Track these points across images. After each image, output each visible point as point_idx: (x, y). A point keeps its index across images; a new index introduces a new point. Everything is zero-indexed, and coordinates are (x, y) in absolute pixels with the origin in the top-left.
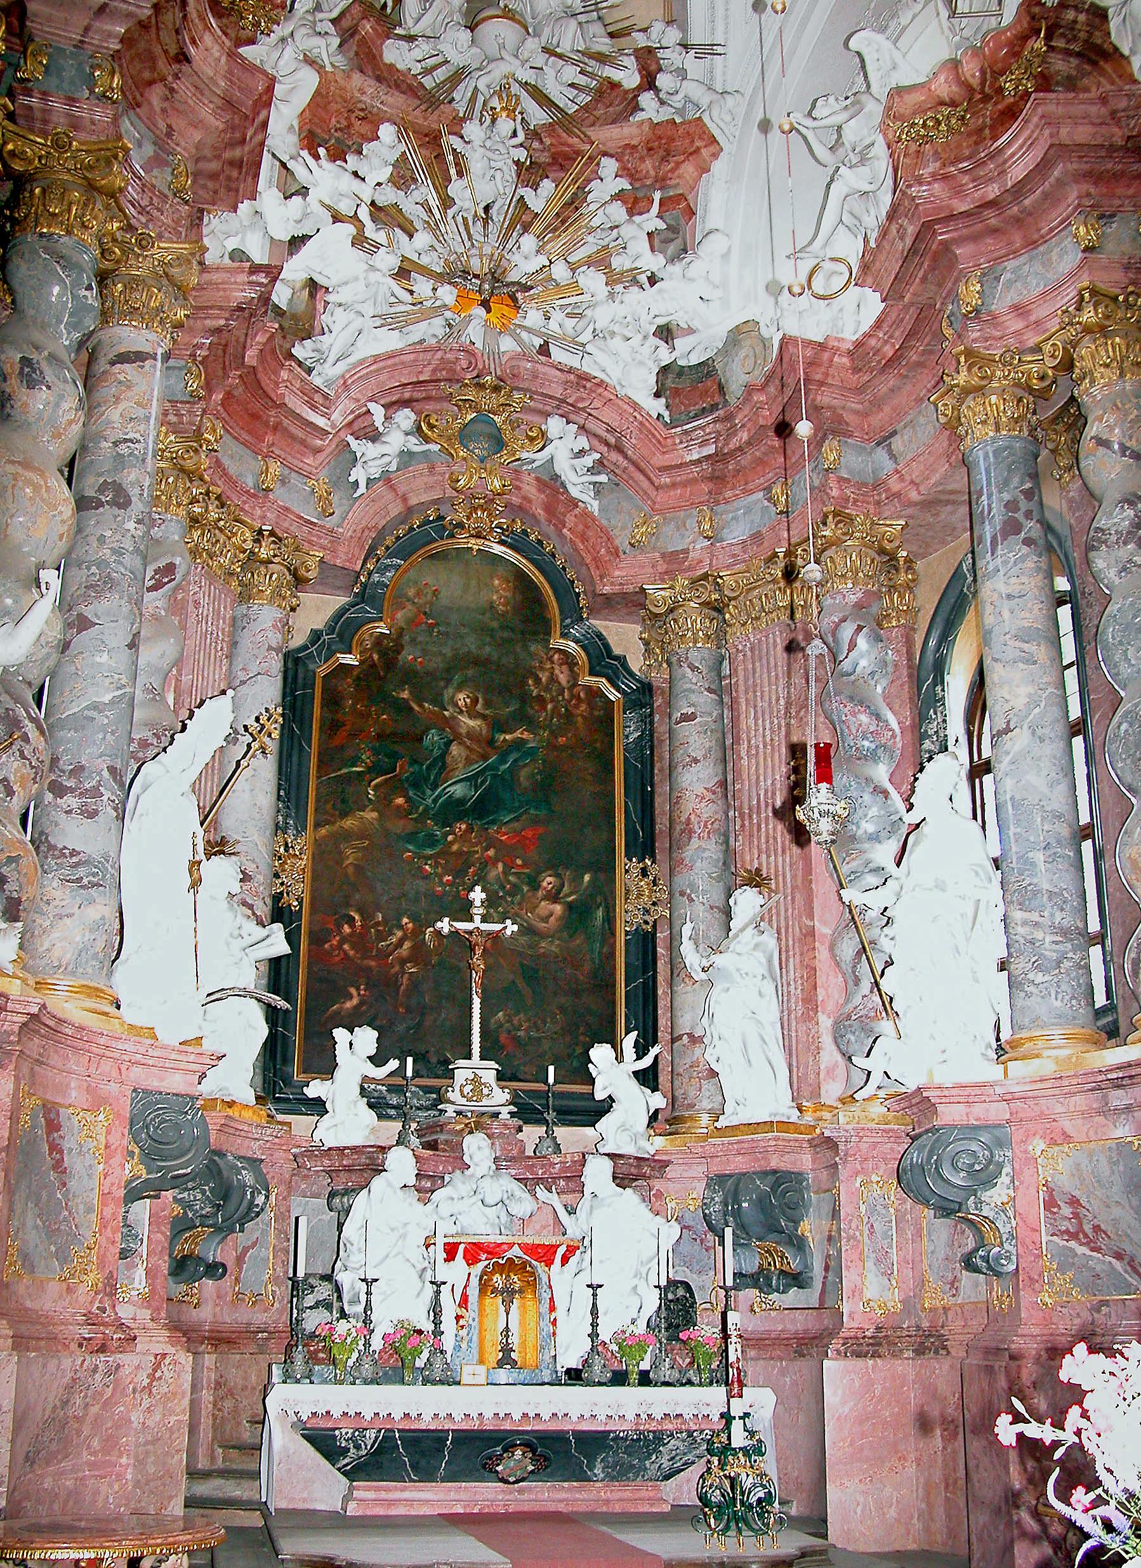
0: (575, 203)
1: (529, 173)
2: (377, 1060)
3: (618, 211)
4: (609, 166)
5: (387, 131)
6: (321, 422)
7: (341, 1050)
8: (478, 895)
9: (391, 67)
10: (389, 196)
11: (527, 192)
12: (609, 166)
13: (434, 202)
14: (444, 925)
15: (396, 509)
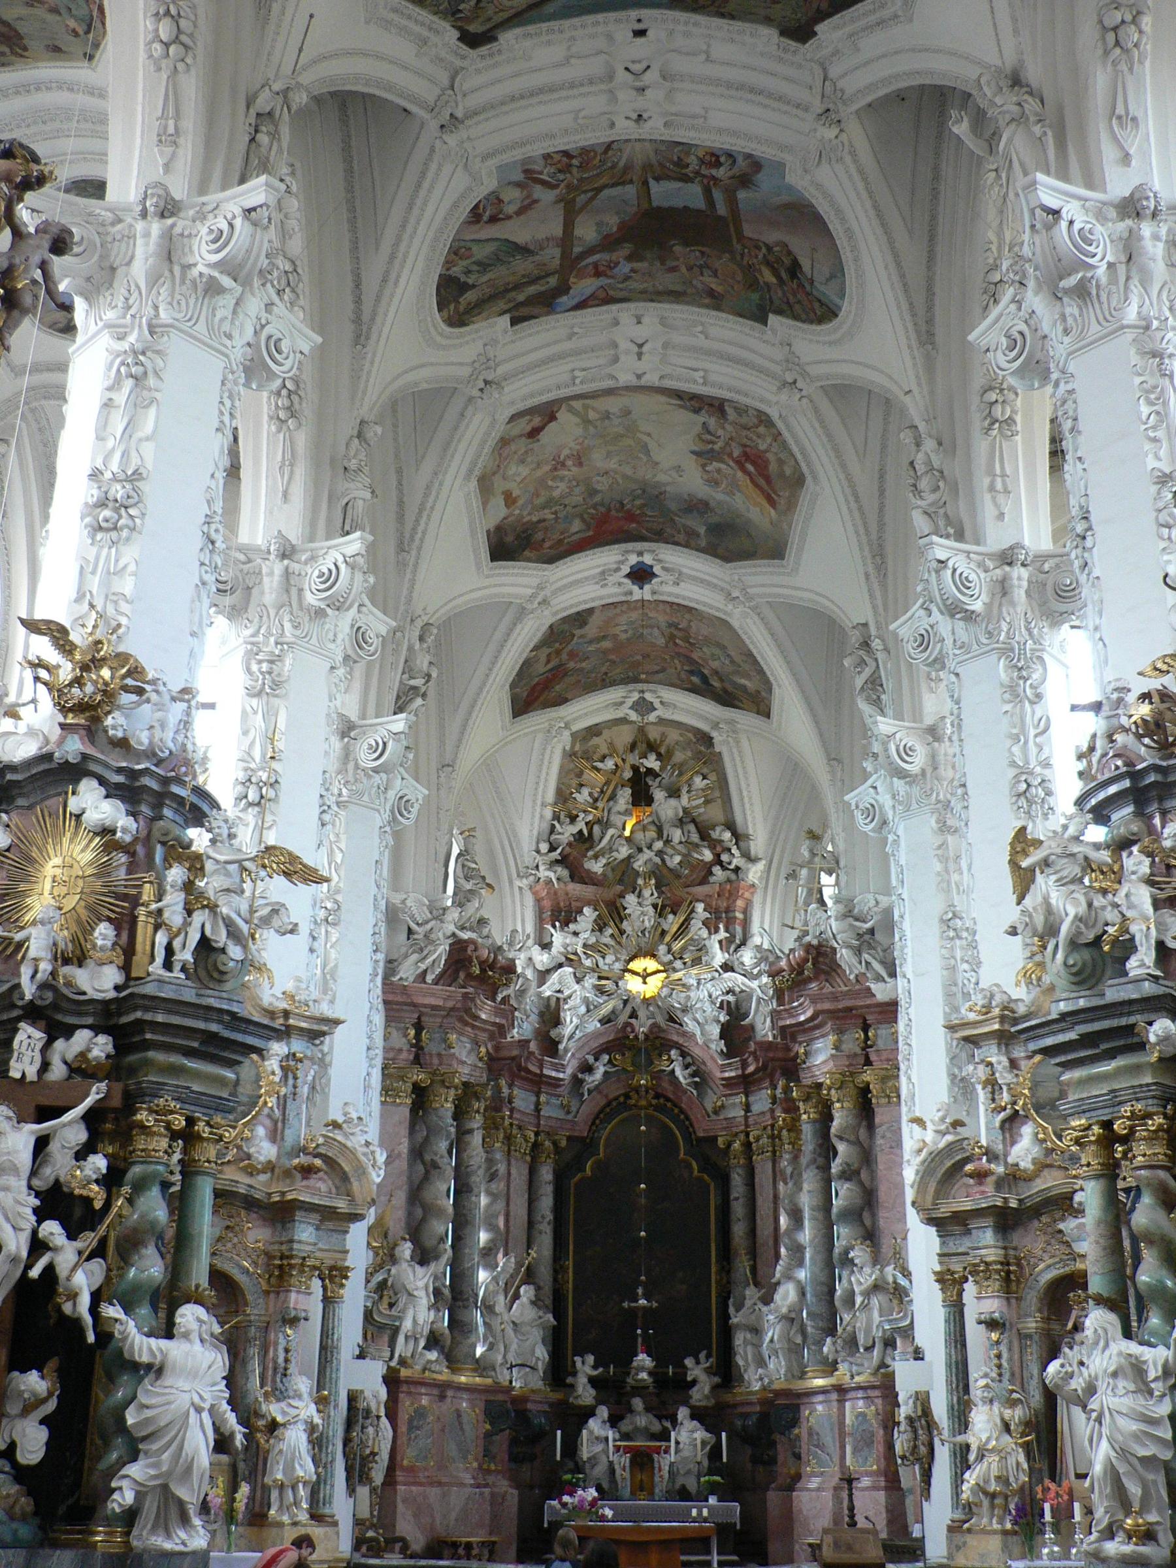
0: (684, 927)
1: (659, 912)
2: (595, 1367)
3: (704, 933)
4: (700, 907)
5: (586, 910)
6: (561, 1076)
7: (579, 1364)
8: (640, 1291)
9: (588, 871)
10: (593, 940)
11: (661, 920)
12: (700, 907)
14: (625, 1305)
15: (603, 1102)
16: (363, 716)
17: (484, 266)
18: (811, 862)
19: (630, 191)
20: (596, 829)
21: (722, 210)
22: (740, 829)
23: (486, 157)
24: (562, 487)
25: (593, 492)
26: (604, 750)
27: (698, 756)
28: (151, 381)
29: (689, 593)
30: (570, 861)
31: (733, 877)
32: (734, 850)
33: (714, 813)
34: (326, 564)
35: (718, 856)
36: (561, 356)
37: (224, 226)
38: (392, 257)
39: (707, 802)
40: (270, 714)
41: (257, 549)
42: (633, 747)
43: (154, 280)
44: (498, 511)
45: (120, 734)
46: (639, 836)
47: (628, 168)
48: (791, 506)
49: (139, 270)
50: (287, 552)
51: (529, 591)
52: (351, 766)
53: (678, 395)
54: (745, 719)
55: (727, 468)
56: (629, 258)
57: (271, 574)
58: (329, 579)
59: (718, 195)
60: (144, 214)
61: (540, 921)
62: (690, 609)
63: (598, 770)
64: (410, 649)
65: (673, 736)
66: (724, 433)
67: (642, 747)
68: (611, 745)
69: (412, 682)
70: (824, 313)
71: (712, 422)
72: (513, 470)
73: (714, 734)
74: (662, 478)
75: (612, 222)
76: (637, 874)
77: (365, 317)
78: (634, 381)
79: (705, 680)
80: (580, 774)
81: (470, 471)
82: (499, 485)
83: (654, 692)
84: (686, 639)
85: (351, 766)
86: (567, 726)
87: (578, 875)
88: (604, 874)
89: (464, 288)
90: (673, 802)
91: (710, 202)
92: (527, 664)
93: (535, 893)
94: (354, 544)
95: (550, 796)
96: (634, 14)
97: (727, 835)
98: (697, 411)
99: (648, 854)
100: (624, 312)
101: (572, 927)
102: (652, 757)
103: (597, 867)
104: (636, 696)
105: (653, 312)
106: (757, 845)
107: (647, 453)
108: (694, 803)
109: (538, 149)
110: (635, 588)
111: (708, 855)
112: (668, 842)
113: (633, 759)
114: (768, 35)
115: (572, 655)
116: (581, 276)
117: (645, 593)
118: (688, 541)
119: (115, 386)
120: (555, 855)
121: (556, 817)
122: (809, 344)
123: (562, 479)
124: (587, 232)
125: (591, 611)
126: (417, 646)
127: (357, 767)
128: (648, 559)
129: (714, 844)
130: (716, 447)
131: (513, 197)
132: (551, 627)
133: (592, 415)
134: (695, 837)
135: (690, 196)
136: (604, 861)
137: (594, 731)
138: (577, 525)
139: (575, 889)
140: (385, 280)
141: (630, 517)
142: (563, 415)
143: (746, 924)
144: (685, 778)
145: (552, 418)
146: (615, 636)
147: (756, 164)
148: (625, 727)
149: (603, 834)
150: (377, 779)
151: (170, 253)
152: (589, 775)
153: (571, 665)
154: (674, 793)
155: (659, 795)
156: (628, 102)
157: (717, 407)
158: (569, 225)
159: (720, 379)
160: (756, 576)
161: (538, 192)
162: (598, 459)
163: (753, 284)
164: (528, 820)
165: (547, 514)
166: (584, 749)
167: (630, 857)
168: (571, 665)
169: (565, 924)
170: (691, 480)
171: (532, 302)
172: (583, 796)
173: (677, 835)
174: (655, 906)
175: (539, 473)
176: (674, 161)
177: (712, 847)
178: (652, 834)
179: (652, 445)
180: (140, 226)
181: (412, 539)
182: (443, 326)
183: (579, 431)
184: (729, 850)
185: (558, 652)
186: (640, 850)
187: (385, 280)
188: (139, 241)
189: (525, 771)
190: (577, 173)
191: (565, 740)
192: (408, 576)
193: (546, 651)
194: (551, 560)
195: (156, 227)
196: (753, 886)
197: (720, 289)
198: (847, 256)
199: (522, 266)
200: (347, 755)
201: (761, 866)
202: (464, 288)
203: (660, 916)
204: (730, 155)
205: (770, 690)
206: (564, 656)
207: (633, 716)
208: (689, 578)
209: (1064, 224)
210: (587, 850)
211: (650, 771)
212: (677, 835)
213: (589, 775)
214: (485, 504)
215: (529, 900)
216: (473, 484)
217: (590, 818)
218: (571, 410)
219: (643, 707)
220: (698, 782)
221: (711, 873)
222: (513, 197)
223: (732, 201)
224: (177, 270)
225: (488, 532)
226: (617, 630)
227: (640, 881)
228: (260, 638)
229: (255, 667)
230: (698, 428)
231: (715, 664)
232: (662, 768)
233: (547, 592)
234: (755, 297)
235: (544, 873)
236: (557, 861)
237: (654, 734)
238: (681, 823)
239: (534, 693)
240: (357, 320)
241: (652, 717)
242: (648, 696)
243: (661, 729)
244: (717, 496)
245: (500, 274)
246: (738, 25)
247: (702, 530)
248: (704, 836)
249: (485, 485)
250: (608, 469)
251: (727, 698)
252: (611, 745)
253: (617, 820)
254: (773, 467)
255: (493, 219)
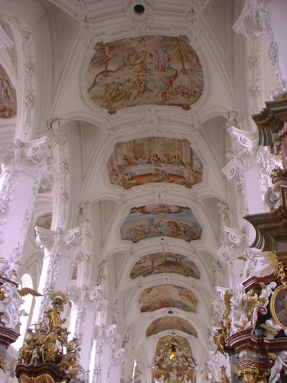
1: (178, 376)
4: (186, 375)
5: (162, 375)
9: (163, 367)
12: (186, 375)
13: (169, 381)
16: (116, 348)
17: (138, 270)
18: (205, 370)
19: (163, 258)
20: (164, 358)
21: (179, 261)
22: (194, 358)
23: (137, 256)
24: (154, 299)
25: (160, 300)
26: (166, 341)
27: (185, 343)
28: (84, 318)
29: (180, 315)
30: (159, 365)
31: (192, 369)
32: (193, 363)
33: (188, 355)
34: (110, 330)
35: (189, 364)
36: (153, 281)
37: (95, 292)
38: (122, 272)
39: (187, 352)
40: (100, 357)
41: (98, 326)
42: (172, 341)
43: (84, 300)
44: (142, 305)
45: (78, 378)
46: (173, 359)
47: (162, 255)
48: (196, 305)
49: (82, 298)
50: (103, 327)
51: (148, 316)
52: (114, 358)
53: (175, 286)
54: (193, 337)
55: (185, 297)
56: (163, 267)
57: (100, 331)
58: (110, 332)
59: (178, 260)
60: (83, 289)
61: (153, 377)
62: (180, 318)
63: (165, 345)
64: (125, 333)
65: (180, 339)
66: (183, 292)
67: (174, 341)
68: (167, 340)
69: (126, 340)
70: (198, 278)
71: (181, 290)
72: (145, 298)
73: (187, 339)
74: (172, 297)
75: (160, 263)
76: (173, 368)
77: (117, 282)
78: (166, 284)
79: (185, 329)
80: (161, 346)
81: (137, 300)
82: (142, 301)
83: (175, 331)
84: (180, 322)
85: (114, 358)
86: (158, 337)
87: (161, 368)
88: (166, 368)
89: (134, 274)
90: (180, 352)
91: (177, 260)
92: (149, 328)
93: (152, 372)
94: (114, 326)
95: (155, 351)
96: (161, 237)
97: (191, 360)
98: (178, 288)
99: (175, 363)
100: (164, 274)
101: (159, 379)
102: (176, 343)
103: (164, 366)
104: (172, 332)
105: (168, 274)
106: (198, 362)
107: (170, 294)
108: (185, 352)
109: (147, 254)
110: (170, 314)
111: (187, 364)
112: (179, 361)
113: (172, 343)
114: (184, 241)
115: (158, 325)
116: (155, 269)
117: (172, 315)
118: (179, 307)
119: (78, 318)
120: (156, 363)
121: (156, 355)
122: (196, 281)
123: (154, 298)
124: (156, 264)
125: (161, 318)
126: (127, 332)
127: (115, 358)
128: (171, 310)
129: (189, 362)
130: (182, 293)
131: (142, 260)
132: (154, 321)
133: (159, 289)
134: (185, 360)
135: (174, 259)
136: (166, 365)
137: (164, 338)
138: (157, 305)
139: (160, 371)
140: (121, 276)
141: (167, 303)
142: (153, 289)
143: (195, 379)
144: (183, 347)
145: (152, 290)
146: (167, 322)
147: (184, 256)
148: (170, 337)
149: (166, 359)
150: (119, 360)
151: (87, 296)
152: (163, 346)
153: (158, 327)
154: (180, 350)
155: (177, 350)
156: (161, 248)
157: (182, 288)
158: (153, 263)
159: (181, 284)
160: (191, 314)
161: (147, 259)
162: (161, 295)
163: (186, 272)
164: (150, 356)
165: (152, 304)
166: (161, 342)
167: (171, 364)
168: (158, 327)
169: (158, 378)
170: (178, 298)
171: (147, 273)
172: (162, 351)
173: (181, 359)
174: (176, 375)
175: (150, 298)
176: (170, 255)
177: (188, 363)
178: (176, 359)
179: (170, 293)
180: (82, 291)
181: (126, 312)
182: (131, 280)
183: (157, 291)
184: (191, 363)
185: (155, 325)
186: (173, 362)
187: (121, 276)
188: (82, 294)
189: (150, 346)
190: (153, 257)
191: (158, 340)
192: (125, 320)
193: (153, 325)
194: (153, 311)
195: (85, 292)
196: (197, 371)
197: (180, 272)
198: (200, 270)
199: (145, 269)
200: (113, 355)
201: (198, 367)
202: (134, 274)
203: (178, 376)
204: (179, 255)
205: (197, 333)
206: (157, 326)
207: (171, 335)
208: (179, 313)
209: (221, 294)
210: (163, 362)
211: (175, 346)
212: (181, 359)
213: (163, 346)
214: (139, 304)
215: (151, 373)
216: (137, 302)
217: (163, 355)
218: (155, 288)
219: (173, 333)
220: (185, 348)
221: (188, 368)
222: (142, 260)
223: (180, 261)
224: (88, 298)
225: (140, 309)
226: (167, 321)
227: (173, 369)
228: (98, 343)
229: (97, 348)
230: (179, 291)
231: (186, 327)
232: (178, 345)
233: (152, 316)
234: (186, 273)
235: (154, 367)
236: (156, 365)
237: (176, 338)
238: (182, 357)
239: (150, 332)
240: (116, 283)
241: (175, 335)
242: (174, 332)
243: (177, 337)
244: (183, 301)
245: (141, 271)
246: (178, 239)
247: (181, 306)
248: (187, 360)
249: (139, 301)
250: (163, 296)
251: (189, 333)
252: (167, 340)
253: (168, 355)
254: (192, 298)
255: (139, 264)
